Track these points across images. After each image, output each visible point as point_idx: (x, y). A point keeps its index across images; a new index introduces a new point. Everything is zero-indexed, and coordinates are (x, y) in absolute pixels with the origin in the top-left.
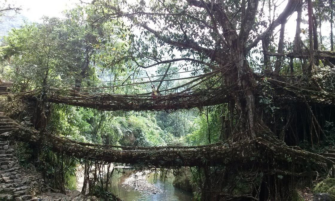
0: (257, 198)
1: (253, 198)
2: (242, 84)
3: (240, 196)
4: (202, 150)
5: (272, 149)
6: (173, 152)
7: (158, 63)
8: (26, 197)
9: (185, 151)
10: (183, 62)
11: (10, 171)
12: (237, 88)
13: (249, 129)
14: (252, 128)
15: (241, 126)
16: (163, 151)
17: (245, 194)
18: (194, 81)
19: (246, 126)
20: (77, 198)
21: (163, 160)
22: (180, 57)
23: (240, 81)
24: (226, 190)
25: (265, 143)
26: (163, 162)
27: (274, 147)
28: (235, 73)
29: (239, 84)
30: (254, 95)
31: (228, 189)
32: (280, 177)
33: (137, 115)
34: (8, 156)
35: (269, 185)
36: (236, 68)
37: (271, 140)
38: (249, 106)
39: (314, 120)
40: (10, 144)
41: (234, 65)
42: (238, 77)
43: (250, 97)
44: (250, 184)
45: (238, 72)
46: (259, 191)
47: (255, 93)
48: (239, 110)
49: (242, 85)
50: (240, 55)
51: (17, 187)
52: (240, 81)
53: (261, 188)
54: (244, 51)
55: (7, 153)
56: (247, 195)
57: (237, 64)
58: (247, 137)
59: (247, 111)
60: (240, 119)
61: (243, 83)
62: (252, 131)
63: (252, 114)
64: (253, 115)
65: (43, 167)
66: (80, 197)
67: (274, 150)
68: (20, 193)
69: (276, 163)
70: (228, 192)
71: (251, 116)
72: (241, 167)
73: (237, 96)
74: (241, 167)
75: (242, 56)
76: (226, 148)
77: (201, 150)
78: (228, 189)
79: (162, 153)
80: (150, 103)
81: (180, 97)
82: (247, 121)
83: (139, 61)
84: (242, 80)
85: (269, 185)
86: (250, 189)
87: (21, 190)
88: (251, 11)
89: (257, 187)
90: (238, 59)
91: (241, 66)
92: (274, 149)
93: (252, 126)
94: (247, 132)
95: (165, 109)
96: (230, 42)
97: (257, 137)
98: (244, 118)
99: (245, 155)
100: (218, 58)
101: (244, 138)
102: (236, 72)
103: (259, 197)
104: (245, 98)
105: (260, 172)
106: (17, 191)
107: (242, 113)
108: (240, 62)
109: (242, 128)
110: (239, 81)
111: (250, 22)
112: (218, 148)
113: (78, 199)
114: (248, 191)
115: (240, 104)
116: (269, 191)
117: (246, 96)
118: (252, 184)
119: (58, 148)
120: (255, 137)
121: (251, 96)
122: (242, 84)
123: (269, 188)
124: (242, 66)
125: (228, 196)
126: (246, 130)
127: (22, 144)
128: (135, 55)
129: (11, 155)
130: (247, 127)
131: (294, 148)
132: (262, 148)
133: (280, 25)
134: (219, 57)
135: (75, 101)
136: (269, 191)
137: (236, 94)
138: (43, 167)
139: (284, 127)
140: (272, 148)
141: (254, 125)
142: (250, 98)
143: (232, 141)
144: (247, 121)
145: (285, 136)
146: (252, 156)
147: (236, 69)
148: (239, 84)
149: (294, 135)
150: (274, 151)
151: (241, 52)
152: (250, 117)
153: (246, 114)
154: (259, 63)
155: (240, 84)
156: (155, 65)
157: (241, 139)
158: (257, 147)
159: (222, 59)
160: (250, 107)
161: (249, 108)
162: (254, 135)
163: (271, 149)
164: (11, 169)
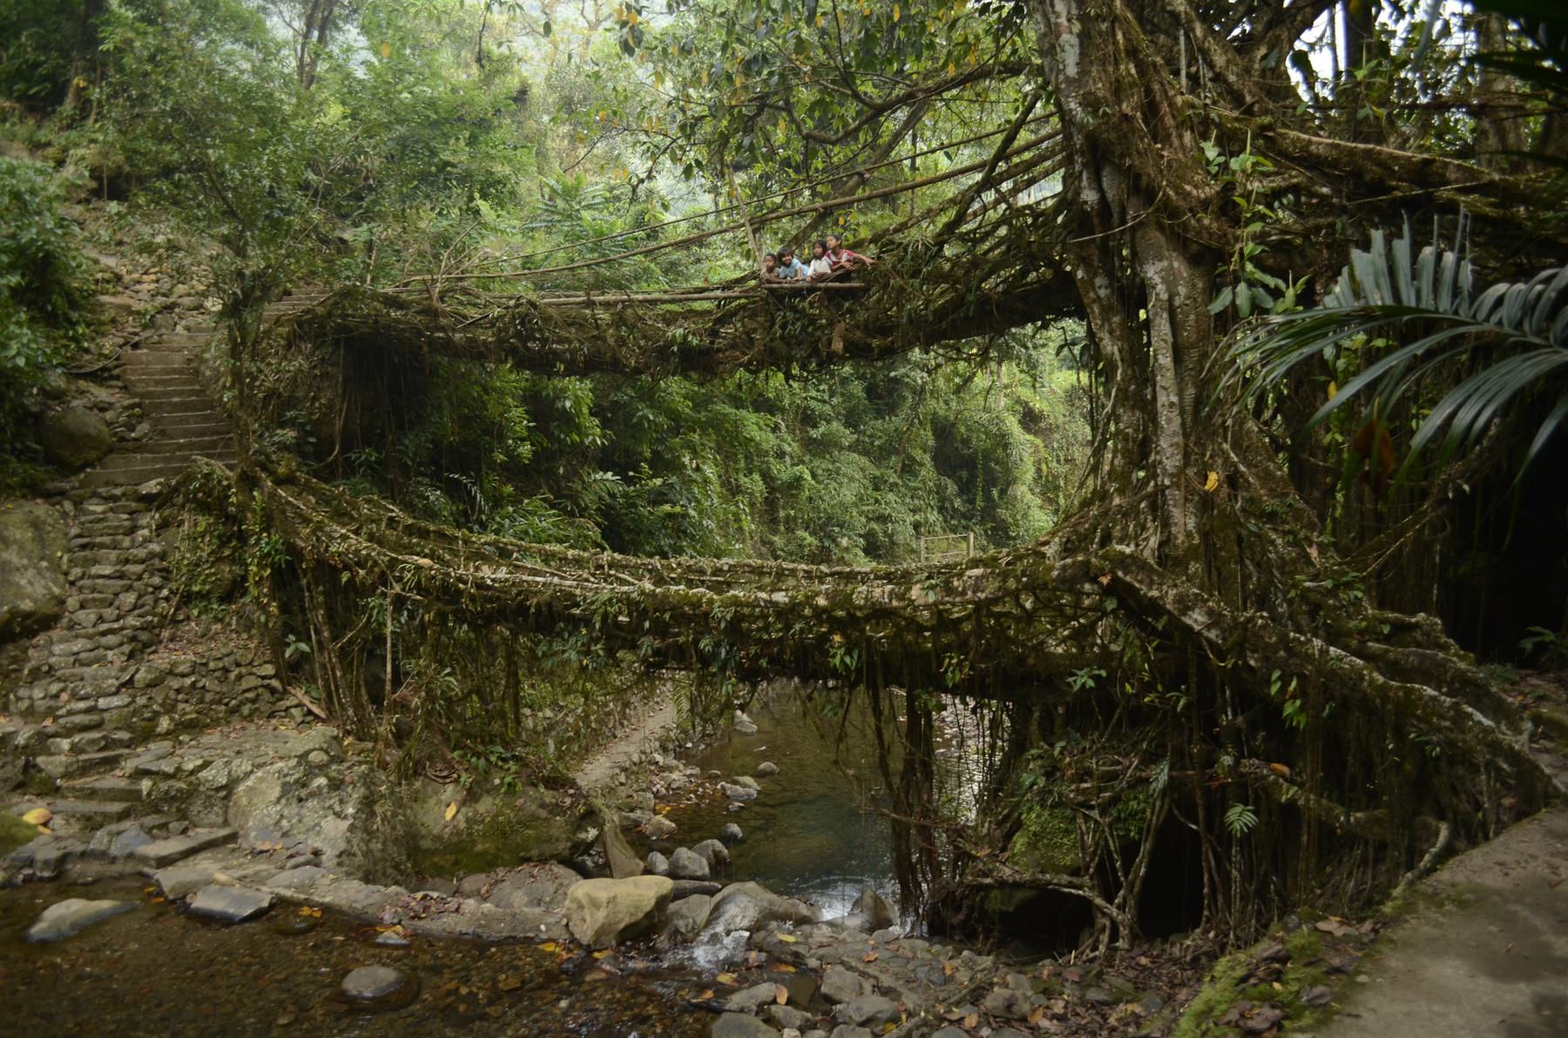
0: (1121, 907)
2: (1101, 190)
3: (1027, 876)
4: (813, 597)
5: (1197, 628)
14: (1172, 475)
23: (1085, 176)
27: (1210, 612)
32: (1240, 818)
44: (1087, 818)
56: (1065, 878)
62: (1173, 496)
67: (1213, 634)
69: (1240, 719)
72: (1061, 710)
74: (1061, 710)
86: (1084, 848)
89: (1129, 850)
91: (1067, 77)
92: (1208, 627)
105: (1151, 759)
112: (891, 592)
120: (1189, 535)
122: (1101, 190)
124: (1072, 71)
127: (203, 522)
140: (1196, 619)
142: (1157, 279)
150: (1209, 641)
163: (1190, 628)
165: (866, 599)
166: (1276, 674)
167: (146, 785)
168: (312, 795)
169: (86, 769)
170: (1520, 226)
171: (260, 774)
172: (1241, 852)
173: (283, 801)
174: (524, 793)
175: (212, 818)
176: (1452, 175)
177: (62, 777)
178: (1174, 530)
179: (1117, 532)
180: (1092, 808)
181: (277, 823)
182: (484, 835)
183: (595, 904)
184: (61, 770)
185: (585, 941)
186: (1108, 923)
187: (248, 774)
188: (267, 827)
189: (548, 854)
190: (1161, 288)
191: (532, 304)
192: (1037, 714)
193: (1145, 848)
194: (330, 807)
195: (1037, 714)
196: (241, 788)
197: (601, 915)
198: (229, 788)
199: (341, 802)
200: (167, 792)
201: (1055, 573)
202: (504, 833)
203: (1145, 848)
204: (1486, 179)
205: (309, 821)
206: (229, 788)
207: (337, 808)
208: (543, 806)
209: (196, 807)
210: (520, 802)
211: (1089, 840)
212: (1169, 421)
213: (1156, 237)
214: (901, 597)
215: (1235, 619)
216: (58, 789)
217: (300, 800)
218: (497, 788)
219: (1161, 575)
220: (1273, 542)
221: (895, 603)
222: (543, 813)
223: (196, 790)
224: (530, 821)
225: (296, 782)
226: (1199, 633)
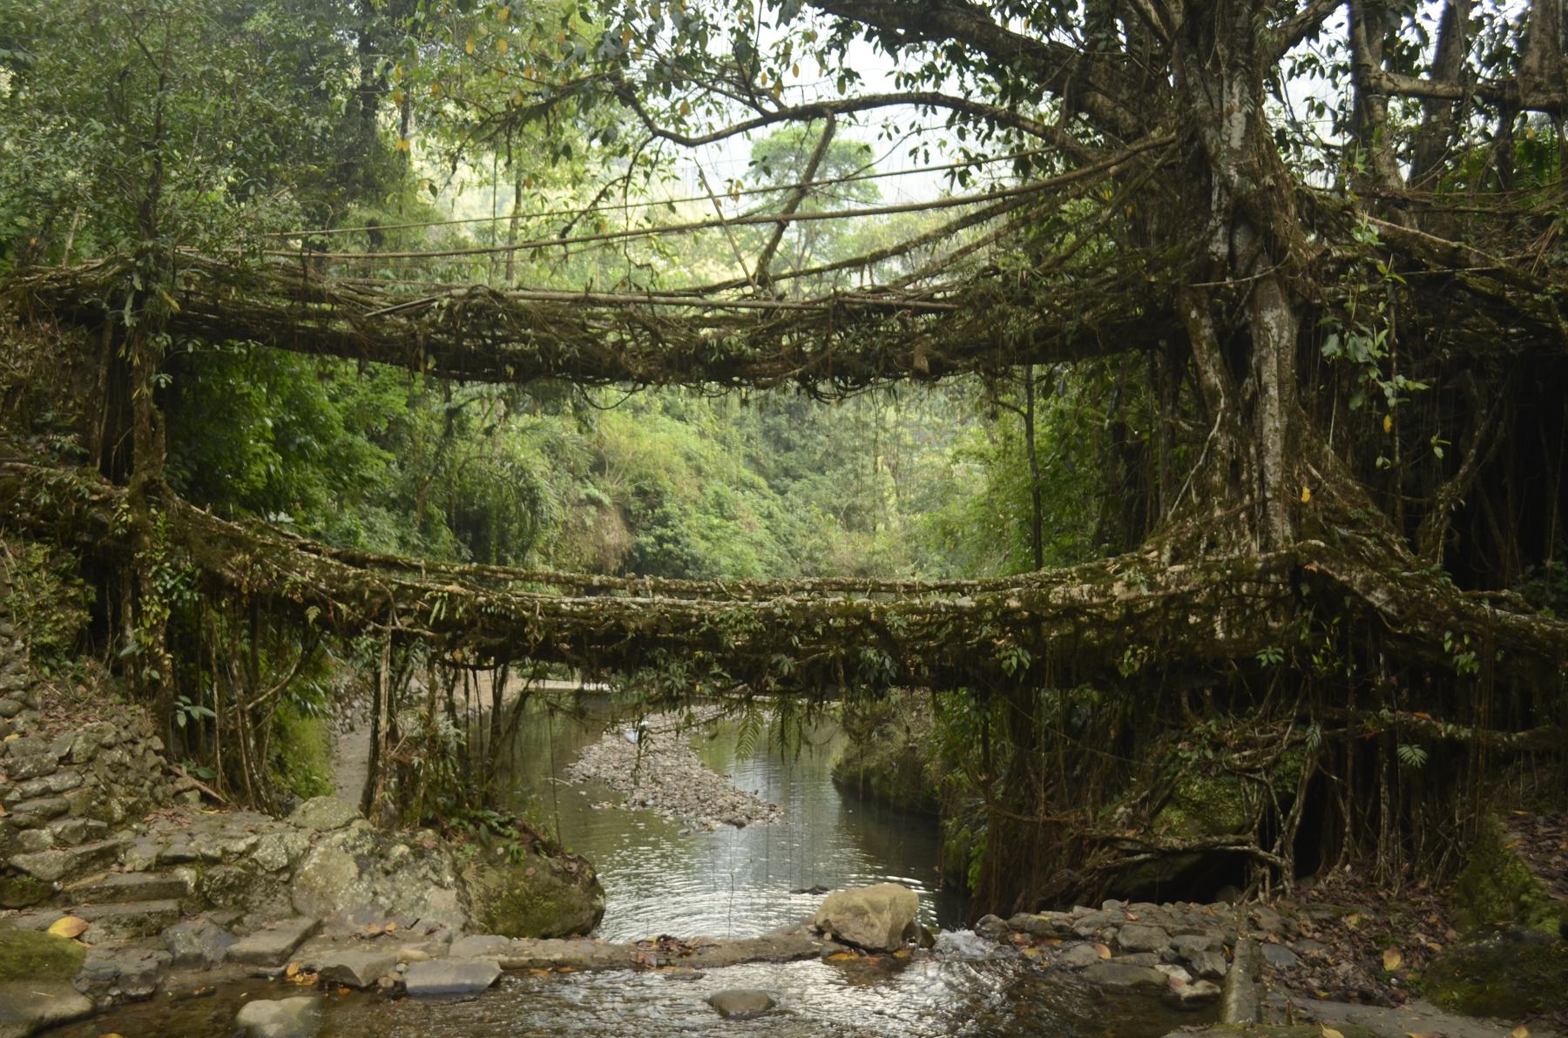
0: (1281, 855)
1: (1262, 853)
3: (1195, 842)
5: (1377, 604)
6: (847, 612)
7: (767, 119)
8: (75, 831)
9: (913, 610)
10: (905, 114)
12: (1208, 268)
13: (1256, 494)
14: (1275, 489)
15: (1217, 478)
16: (789, 607)
17: (1219, 831)
18: (966, 222)
19: (1244, 476)
20: (340, 836)
21: (793, 652)
22: (887, 87)
23: (1221, 231)
24: (1121, 809)
25: (1342, 569)
26: (788, 665)
27: (1390, 592)
28: (1196, 185)
29: (1213, 248)
30: (1295, 311)
31: (1134, 807)
32: (1412, 754)
33: (637, 410)
35: (1350, 793)
36: (1203, 150)
37: (1376, 555)
38: (1264, 368)
41: (1192, 139)
42: (1214, 207)
43: (1276, 323)
44: (1251, 780)
45: (1216, 179)
46: (1294, 818)
47: (1299, 300)
48: (1209, 389)
49: (1232, 254)
50: (1226, 83)
51: (27, 778)
52: (1221, 231)
53: (1307, 805)
54: (1249, 62)
56: (1232, 838)
57: (1209, 133)
58: (1243, 536)
59: (1254, 395)
60: (1215, 441)
61: (1239, 239)
62: (1275, 508)
63: (1281, 413)
64: (1285, 419)
65: (156, 675)
66: (354, 832)
67: (1390, 609)
68: (42, 807)
69: (1393, 679)
70: (1132, 823)
71: (1272, 422)
72: (1208, 693)
73: (1202, 315)
74: (1208, 693)
75: (1236, 90)
76: (1132, 594)
77: (998, 603)
78: (1134, 807)
79: (785, 616)
80: (720, 341)
81: (889, 310)
82: (1252, 450)
83: (656, 103)
84: (1231, 226)
85: (1350, 793)
86: (1250, 808)
87: (46, 792)
89: (1287, 802)
90: (1216, 106)
92: (1387, 603)
93: (1273, 479)
94: (1250, 510)
95: (802, 379)
96: (1173, 7)
97: (1299, 536)
98: (1235, 435)
99: (1228, 632)
100: (1100, 98)
101: (1231, 545)
102: (1204, 181)
103: (1291, 849)
104: (1246, 326)
105: (1303, 721)
106: (25, 797)
107: (1226, 409)
108: (1226, 122)
109: (1223, 489)
110: (1217, 228)
112: (1090, 591)
113: (344, 843)
114: (1235, 821)
115: (1217, 355)
116: (1348, 820)
118: (1261, 783)
119: (233, 581)
120: (1286, 539)
121: (1276, 312)
123: (1344, 808)
124: (1236, 143)
125: (1128, 840)
126: (1241, 497)
127: (38, 553)
128: (635, 72)
130: (1250, 481)
131: (1496, 602)
132: (1328, 596)
134: (1105, 94)
135: (310, 324)
136: (1348, 820)
137: (1197, 304)
138: (156, 675)
139: (1447, 486)
140: (1378, 597)
141: (1287, 477)
142: (1273, 324)
143: (1165, 558)
144: (1252, 450)
145: (1449, 534)
146: (1268, 638)
147: (1202, 163)
148: (1213, 248)
150: (1385, 614)
151: (1233, 67)
152: (1266, 430)
153: (1250, 410)
154: (1324, 129)
155: (1220, 248)
156: (744, 128)
157: (1212, 544)
158: (1297, 591)
159: (1125, 104)
160: (1269, 374)
161: (1265, 377)
162: (1282, 528)
163: (1371, 605)
165: (1064, 598)
166: (1448, 635)
167: (186, 875)
168: (399, 865)
169: (84, 865)
170: (1508, 303)
171: (321, 849)
172: (1389, 789)
173: (366, 877)
174: (532, 862)
175: (277, 908)
176: (1473, 261)
177: (58, 879)
178: (1274, 535)
179: (1222, 538)
180: (1259, 770)
181: (373, 902)
182: (504, 913)
183: (878, 909)
184: (59, 868)
185: (882, 942)
186: (1267, 871)
187: (307, 850)
188: (363, 907)
189: (570, 926)
190: (1275, 331)
191: (495, 295)
192: (1184, 700)
193: (1298, 802)
194: (425, 877)
195: (1184, 700)
196: (308, 867)
197: (887, 916)
198: (291, 867)
199: (434, 870)
200: (224, 881)
201: (1259, 565)
202: (524, 909)
203: (1298, 802)
204: (1496, 266)
205: (409, 893)
206: (291, 867)
207: (431, 874)
208: (554, 873)
209: (257, 897)
210: (530, 871)
211: (1254, 799)
212: (1274, 443)
213: (1275, 288)
214: (1103, 594)
215: (1410, 595)
216: (55, 893)
217: (387, 873)
218: (502, 857)
219: (1349, 563)
220: (1364, 543)
221: (1095, 600)
222: (558, 881)
223: (254, 874)
224: (546, 891)
225: (371, 853)
226: (1379, 609)
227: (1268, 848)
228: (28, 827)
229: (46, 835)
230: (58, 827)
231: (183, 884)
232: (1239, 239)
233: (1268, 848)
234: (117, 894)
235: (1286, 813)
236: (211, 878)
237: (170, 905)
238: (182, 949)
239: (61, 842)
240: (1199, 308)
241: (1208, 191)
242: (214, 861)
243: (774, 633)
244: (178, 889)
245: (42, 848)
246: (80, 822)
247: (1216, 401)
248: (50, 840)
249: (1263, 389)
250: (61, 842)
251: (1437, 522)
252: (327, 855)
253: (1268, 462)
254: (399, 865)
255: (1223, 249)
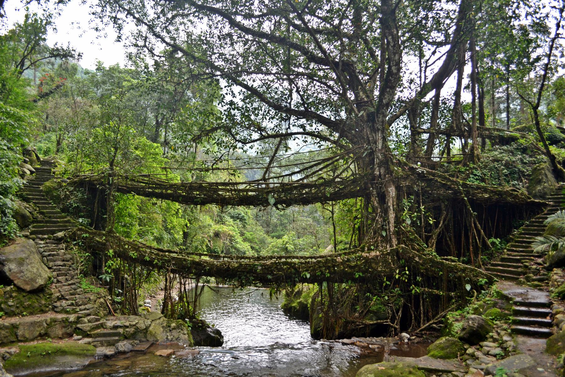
0: (397, 325)
11: (69, 285)
20: (158, 321)
29: (375, 173)
34: (65, 265)
39: (475, 224)
40: (66, 249)
43: (392, 191)
51: (80, 305)
55: (63, 261)
75: (380, 135)
84: (380, 167)
87: (85, 309)
88: (392, 77)
89: (397, 312)
93: (392, 229)
97: (399, 243)
103: (399, 323)
111: (391, 91)
117: (385, 189)
123: (412, 313)
124: (380, 148)
129: (70, 263)
133: (434, 90)
135: (150, 190)
148: (375, 173)
149: (449, 242)
153: (386, 211)
160: (390, 204)
161: (389, 204)
162: (395, 241)
164: (70, 282)
187: (150, 325)
193: (400, 312)
196: (151, 329)
198: (147, 328)
203: (400, 312)
206: (147, 328)
227: (393, 323)
228: (81, 317)
229: (86, 320)
230: (89, 318)
231: (120, 333)
232: (382, 171)
233: (393, 323)
234: (105, 335)
235: (397, 314)
236: (127, 331)
237: (117, 338)
238: (121, 349)
239: (89, 321)
240: (373, 188)
241: (373, 159)
242: (127, 327)
243: (267, 269)
244: (118, 334)
245: (85, 323)
246: (94, 317)
247: (377, 209)
248: (87, 321)
249: (389, 207)
250: (89, 321)
251: (434, 241)
252: (155, 326)
253: (391, 225)
254: (174, 329)
255: (378, 173)
